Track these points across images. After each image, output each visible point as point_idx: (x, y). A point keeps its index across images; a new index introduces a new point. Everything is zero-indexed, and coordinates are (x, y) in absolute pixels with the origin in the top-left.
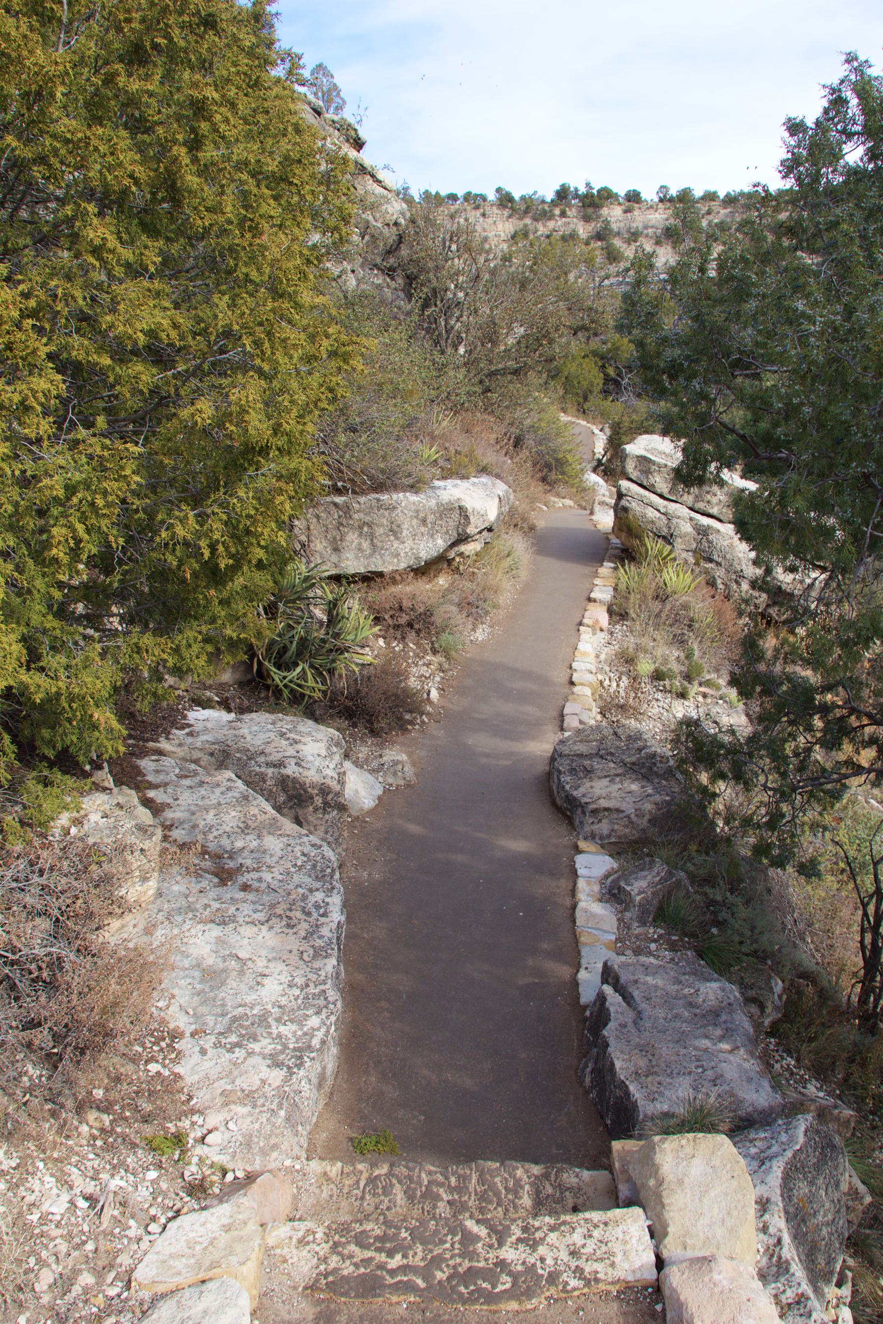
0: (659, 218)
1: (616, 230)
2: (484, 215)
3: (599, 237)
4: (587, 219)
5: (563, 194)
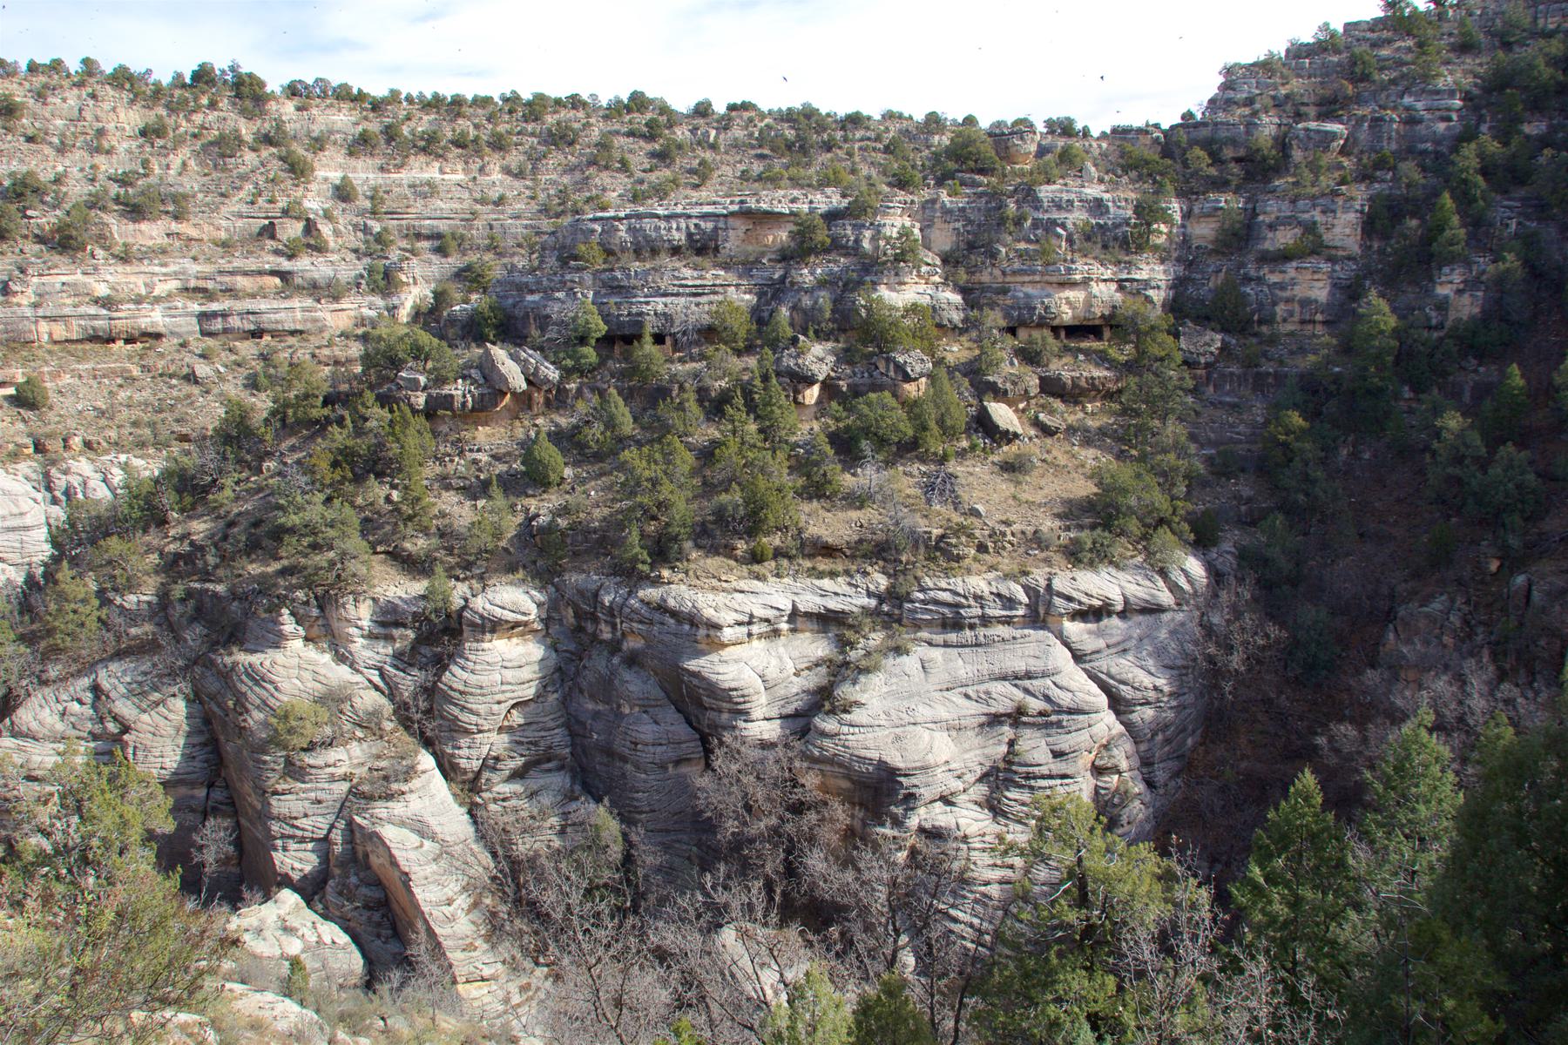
2: (93, 96)
3: (267, 140)
4: (250, 117)
5: (203, 76)
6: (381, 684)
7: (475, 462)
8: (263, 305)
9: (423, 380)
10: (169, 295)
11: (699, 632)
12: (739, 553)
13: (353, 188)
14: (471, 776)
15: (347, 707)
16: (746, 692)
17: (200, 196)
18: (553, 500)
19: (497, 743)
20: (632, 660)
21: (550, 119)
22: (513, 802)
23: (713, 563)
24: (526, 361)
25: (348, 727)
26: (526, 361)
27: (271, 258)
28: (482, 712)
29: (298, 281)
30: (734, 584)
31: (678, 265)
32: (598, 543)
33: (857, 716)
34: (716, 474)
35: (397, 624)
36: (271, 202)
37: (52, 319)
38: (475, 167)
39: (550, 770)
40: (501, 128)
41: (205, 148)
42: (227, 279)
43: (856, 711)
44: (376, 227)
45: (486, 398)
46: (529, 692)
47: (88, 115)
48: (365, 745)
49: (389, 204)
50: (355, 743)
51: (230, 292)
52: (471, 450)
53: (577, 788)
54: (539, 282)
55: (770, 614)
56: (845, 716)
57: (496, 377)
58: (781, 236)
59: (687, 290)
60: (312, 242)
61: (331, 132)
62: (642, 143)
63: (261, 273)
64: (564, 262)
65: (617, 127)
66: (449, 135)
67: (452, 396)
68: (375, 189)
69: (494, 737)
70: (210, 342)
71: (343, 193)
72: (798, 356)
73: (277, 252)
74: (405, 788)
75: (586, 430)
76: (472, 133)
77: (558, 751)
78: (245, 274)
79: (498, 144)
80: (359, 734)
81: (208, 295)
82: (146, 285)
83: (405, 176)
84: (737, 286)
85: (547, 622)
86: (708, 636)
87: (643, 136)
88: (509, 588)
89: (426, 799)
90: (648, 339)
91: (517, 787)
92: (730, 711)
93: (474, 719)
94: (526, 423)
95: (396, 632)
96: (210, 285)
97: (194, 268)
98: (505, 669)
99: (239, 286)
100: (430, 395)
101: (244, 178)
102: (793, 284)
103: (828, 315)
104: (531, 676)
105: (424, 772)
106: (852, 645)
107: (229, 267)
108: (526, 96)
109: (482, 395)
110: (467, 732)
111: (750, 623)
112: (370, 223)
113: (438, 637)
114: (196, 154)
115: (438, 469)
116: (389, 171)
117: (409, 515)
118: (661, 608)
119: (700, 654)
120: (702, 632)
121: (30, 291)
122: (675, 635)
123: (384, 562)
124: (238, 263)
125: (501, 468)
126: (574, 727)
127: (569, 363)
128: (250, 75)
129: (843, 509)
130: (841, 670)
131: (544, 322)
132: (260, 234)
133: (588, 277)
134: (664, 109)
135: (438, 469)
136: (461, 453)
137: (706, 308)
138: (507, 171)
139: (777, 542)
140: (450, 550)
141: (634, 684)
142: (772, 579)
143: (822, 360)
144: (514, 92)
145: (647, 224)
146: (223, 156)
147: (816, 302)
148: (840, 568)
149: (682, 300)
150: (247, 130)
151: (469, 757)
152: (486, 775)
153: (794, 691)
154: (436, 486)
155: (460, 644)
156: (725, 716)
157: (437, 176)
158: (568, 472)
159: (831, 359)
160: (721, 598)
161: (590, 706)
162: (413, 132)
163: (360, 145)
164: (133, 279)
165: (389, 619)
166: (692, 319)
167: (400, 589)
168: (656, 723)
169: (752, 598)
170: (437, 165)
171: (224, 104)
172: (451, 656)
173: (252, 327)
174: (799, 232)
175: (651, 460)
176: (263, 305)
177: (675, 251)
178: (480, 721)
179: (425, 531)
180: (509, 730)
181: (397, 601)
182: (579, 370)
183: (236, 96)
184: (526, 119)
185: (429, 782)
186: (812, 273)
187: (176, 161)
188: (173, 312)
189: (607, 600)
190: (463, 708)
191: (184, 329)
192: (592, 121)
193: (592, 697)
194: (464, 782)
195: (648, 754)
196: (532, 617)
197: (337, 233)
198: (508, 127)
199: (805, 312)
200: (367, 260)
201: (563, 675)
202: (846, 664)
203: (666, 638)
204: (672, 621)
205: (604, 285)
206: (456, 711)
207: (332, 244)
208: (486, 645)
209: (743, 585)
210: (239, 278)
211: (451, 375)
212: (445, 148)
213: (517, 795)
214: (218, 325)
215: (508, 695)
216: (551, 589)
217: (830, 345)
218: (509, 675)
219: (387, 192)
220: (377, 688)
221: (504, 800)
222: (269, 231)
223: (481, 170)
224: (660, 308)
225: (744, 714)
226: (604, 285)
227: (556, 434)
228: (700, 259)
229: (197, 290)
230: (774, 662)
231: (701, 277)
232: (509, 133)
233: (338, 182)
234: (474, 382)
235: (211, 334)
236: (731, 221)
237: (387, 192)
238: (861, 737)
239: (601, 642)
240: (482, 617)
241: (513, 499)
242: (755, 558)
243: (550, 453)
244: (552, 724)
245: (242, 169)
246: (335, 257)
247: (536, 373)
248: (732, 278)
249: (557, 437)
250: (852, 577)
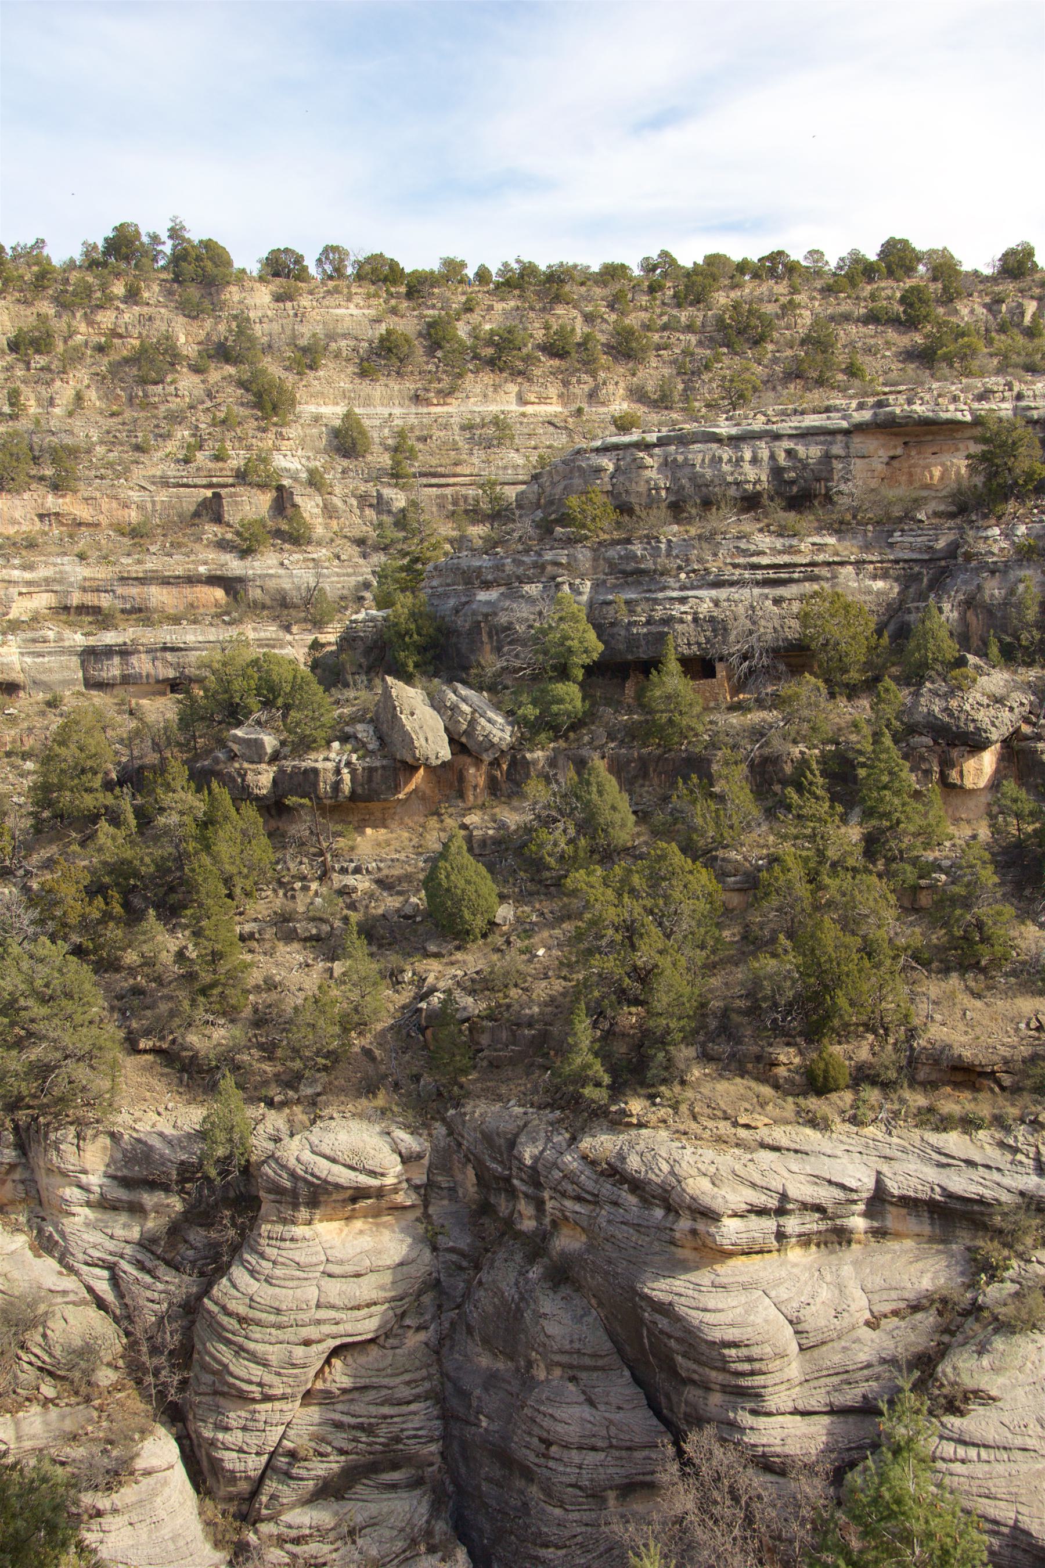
0: (355, 314)
1: (265, 340)
3: (223, 353)
4: (191, 311)
5: (123, 246)
6: (109, 1296)
7: (344, 892)
8: (190, 635)
9: (270, 742)
10: (35, 619)
11: (679, 1225)
12: (782, 1071)
13: (363, 433)
14: (244, 1487)
15: (34, 1337)
16: (755, 1351)
17: (100, 450)
18: (473, 960)
19: (294, 1422)
20: (562, 1275)
21: (721, 299)
22: (312, 1548)
23: (730, 1090)
24: (454, 708)
25: (28, 1375)
26: (454, 708)
27: (211, 555)
28: (274, 1360)
29: (255, 593)
30: (763, 1133)
31: (747, 527)
32: (525, 1047)
33: (976, 1422)
34: (765, 916)
35: (152, 1185)
36: (218, 458)
38: (580, 390)
39: (393, 1487)
40: (634, 320)
41: (115, 368)
42: (134, 591)
43: (977, 1410)
44: (399, 500)
45: (378, 776)
46: (367, 1325)
48: (54, 1412)
49: (425, 459)
50: (35, 1408)
51: (140, 613)
52: (344, 871)
53: (441, 1527)
54: (499, 568)
55: (825, 1195)
56: (951, 1420)
57: (396, 737)
58: (952, 467)
59: (759, 575)
60: (285, 527)
61: (332, 337)
62: (891, 334)
63: (191, 580)
64: (546, 528)
65: (844, 308)
66: (539, 335)
67: (315, 771)
68: (401, 434)
69: (293, 1409)
70: (98, 698)
71: (346, 442)
72: (951, 693)
73: (222, 545)
74: (103, 1502)
75: (543, 834)
76: (580, 328)
77: (413, 1447)
78: (166, 582)
79: (625, 349)
80: (48, 1390)
81: (100, 618)
83: (455, 410)
84: (859, 564)
85: (426, 1191)
86: (694, 1232)
87: (895, 322)
88: (354, 1124)
89: (143, 1531)
90: (673, 666)
91: (320, 1516)
92: (726, 1389)
93: (257, 1372)
94: (449, 822)
95: (149, 1199)
96: (105, 601)
97: (78, 572)
98: (332, 1275)
99: (153, 603)
100: (281, 771)
101: (175, 418)
102: (968, 557)
103: (1032, 614)
104: (374, 1295)
105: (148, 1473)
106: (993, 1272)
107: (137, 570)
108: (689, 255)
109: (370, 770)
110: (243, 1398)
111: (781, 1212)
112: (388, 492)
113: (219, 1209)
114: (99, 379)
115: (279, 902)
116: (428, 403)
117: (206, 984)
118: (614, 1172)
119: (678, 1267)
120: (684, 1224)
122: (637, 1227)
123: (149, 1068)
124: (152, 564)
125: (391, 903)
126: (450, 1403)
127: (531, 711)
128: (209, 245)
129: (1009, 993)
130: (960, 1320)
131: (503, 636)
132: (197, 514)
133: (583, 555)
134: (944, 268)
135: (279, 902)
136: (323, 877)
137: (796, 607)
138: (638, 395)
139: (863, 1054)
140: (269, 1051)
141: (558, 1321)
142: (840, 1127)
143: (998, 701)
144: (664, 254)
145: (698, 454)
146: (143, 381)
147: (1012, 592)
148: (985, 1110)
149: (746, 595)
150: (186, 336)
151: (241, 1450)
152: (271, 1486)
153: (863, 1357)
154: (269, 933)
155: (254, 1222)
156: (716, 1399)
157: (514, 408)
158: (505, 912)
159: (1021, 699)
160: (729, 1160)
161: (484, 1361)
162: (474, 334)
163: (382, 357)
165: (137, 1174)
166: (766, 629)
167: (159, 1116)
168: (591, 1403)
169: (794, 1163)
170: (513, 388)
171: (152, 293)
172: (235, 1249)
173: (171, 674)
174: (984, 457)
175: (625, 889)
176: (190, 635)
177: (750, 503)
178: (268, 1378)
179: (230, 1014)
180: (326, 1398)
181: (156, 1143)
182: (545, 725)
183: (176, 280)
184: (679, 301)
185: (154, 1494)
186: (1007, 535)
187: (64, 392)
188: (39, 647)
189: (528, 1153)
190: (240, 1350)
191: (56, 677)
192: (801, 298)
193: (486, 1341)
194: (230, 1499)
195: (575, 1467)
196: (390, 1180)
197: (329, 511)
198: (643, 315)
199: (989, 610)
200: (379, 558)
201: (439, 1300)
202: (975, 1309)
203: (621, 1233)
204: (633, 1199)
205: (613, 568)
206: (225, 1354)
207: (319, 531)
208: (299, 1231)
209: (779, 1135)
210: (154, 590)
211: (320, 734)
212: (528, 359)
213: (320, 1533)
214: (113, 669)
215: (327, 1329)
216: (440, 1129)
217: (1032, 674)
218: (334, 1290)
219: (424, 439)
220: (101, 1304)
221: (297, 1541)
222: (212, 509)
223: (592, 396)
224: (705, 608)
225: (750, 1397)
226: (613, 568)
227: (497, 842)
228: (792, 515)
229: (82, 609)
230: (825, 1293)
231: (790, 550)
232: (647, 327)
233: (337, 423)
234: (360, 746)
235: (101, 685)
236: (858, 442)
237: (424, 439)
238: (980, 1470)
239: (518, 1235)
240: (293, 1175)
241: (393, 959)
242: (816, 1083)
243: (473, 879)
244: (405, 1392)
245: (174, 404)
246: (323, 553)
247: (470, 732)
248: (849, 549)
249: (478, 848)
250: (1007, 1129)
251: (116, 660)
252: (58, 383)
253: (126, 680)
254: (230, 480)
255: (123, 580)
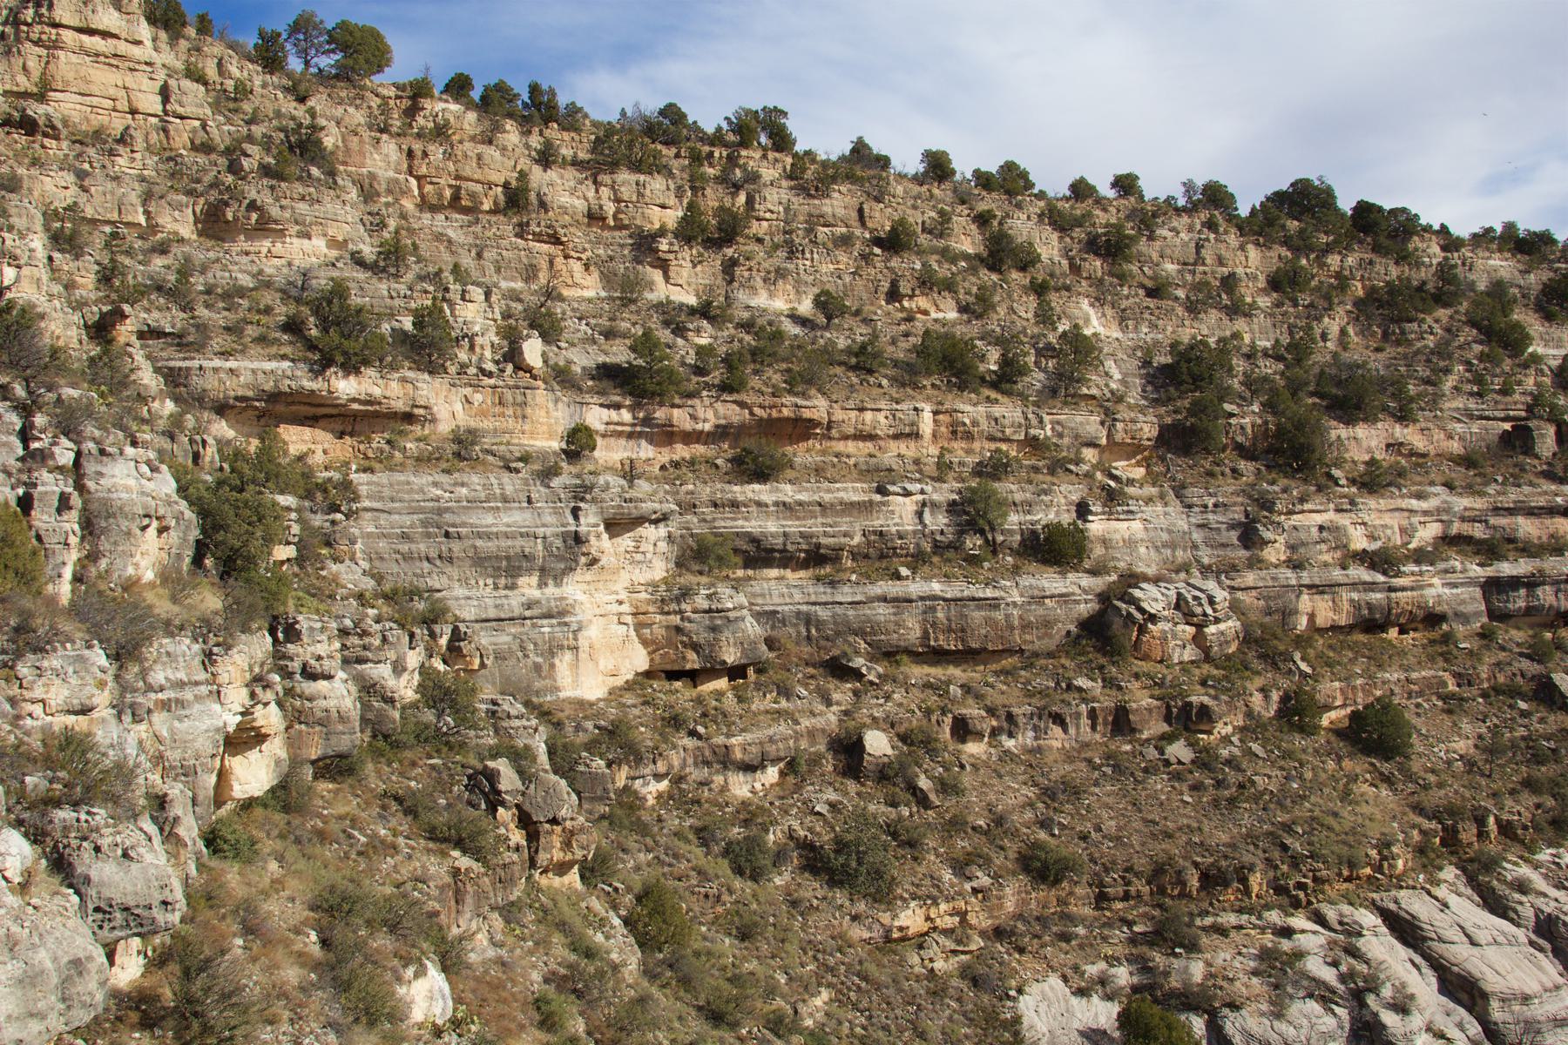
37: (1316, 589)
47: (1208, 254)
78: (1531, 512)
82: (1403, 530)
96: (1478, 531)
97: (1462, 503)
99: (1521, 534)
121: (1281, 539)
164: (1388, 519)
188: (1451, 578)
210: (1520, 520)
214: (1519, 600)
251: (1523, 592)
252: (1326, 320)
253: (1529, 611)
254: (1523, 414)
255: (1497, 510)
